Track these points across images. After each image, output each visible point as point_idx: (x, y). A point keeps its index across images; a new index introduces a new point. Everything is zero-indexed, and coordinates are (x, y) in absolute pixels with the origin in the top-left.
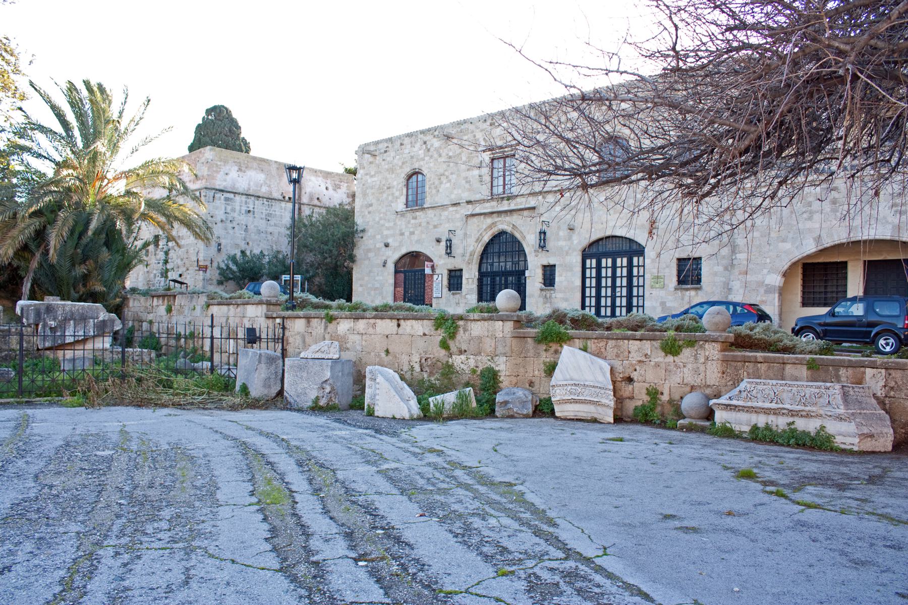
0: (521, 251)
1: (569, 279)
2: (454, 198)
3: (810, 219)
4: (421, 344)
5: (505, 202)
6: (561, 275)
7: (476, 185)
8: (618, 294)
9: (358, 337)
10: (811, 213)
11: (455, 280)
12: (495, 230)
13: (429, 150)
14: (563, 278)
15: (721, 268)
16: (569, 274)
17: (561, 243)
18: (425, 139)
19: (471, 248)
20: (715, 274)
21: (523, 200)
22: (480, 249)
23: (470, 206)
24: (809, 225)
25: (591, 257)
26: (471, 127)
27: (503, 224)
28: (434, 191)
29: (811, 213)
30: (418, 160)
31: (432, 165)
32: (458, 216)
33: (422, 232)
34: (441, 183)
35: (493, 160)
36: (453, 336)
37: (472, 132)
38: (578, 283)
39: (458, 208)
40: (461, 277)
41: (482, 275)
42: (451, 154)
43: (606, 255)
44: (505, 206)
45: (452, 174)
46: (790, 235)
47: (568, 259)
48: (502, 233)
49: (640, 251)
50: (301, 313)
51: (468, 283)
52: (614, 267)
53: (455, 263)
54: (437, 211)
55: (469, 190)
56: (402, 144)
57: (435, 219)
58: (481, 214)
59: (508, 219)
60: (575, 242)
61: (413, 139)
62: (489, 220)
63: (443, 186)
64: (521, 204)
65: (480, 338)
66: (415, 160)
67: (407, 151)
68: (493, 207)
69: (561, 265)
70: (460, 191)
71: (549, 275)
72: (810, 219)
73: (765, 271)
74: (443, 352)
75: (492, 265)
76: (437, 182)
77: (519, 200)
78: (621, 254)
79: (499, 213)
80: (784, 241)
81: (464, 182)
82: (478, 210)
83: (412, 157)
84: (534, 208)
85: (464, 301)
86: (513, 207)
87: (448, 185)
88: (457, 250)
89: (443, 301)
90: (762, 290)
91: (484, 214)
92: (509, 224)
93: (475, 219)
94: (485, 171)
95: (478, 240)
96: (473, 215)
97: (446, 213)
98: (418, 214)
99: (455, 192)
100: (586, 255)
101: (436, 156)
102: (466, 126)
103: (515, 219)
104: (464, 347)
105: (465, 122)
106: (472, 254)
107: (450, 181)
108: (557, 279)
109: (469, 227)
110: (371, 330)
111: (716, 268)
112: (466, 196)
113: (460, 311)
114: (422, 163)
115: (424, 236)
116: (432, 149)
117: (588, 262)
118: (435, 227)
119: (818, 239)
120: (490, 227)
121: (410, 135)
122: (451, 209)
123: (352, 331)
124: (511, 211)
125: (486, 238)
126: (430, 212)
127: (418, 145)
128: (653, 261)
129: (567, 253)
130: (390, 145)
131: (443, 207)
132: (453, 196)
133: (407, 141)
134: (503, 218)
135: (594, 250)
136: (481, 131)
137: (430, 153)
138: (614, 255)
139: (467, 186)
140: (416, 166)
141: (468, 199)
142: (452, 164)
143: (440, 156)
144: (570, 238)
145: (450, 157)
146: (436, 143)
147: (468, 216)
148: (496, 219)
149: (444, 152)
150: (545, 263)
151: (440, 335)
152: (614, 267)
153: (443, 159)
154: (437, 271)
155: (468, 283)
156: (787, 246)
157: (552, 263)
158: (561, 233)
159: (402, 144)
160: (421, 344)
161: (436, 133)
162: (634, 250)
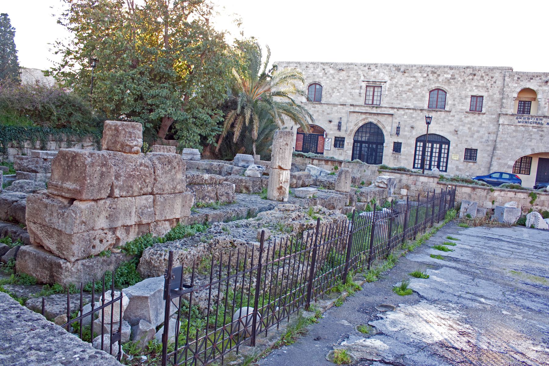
0: (382, 135)
1: (408, 150)
2: (342, 100)
3: (530, 141)
4: (522, 201)
5: (374, 109)
6: (405, 148)
7: (357, 97)
8: (433, 160)
9: (501, 198)
10: (531, 139)
11: (339, 142)
12: (366, 121)
13: (326, 74)
14: (405, 149)
15: (486, 155)
16: (409, 148)
17: (406, 133)
18: (324, 67)
19: (352, 128)
20: (484, 157)
21: (385, 109)
22: (356, 129)
23: (352, 107)
24: (530, 143)
25: (420, 141)
26: (356, 68)
27: (373, 119)
28: (328, 96)
29: (531, 139)
30: (318, 77)
31: (328, 82)
32: (344, 111)
33: (319, 115)
34: (334, 92)
35: (367, 86)
36: (534, 200)
37: (356, 70)
38: (413, 153)
39: (344, 107)
40: (344, 141)
41: (355, 141)
42: (341, 78)
43: (429, 142)
44: (374, 111)
45: (341, 89)
46: (521, 146)
47: (409, 141)
48: (371, 123)
49: (448, 142)
50: (471, 185)
51: (348, 145)
52: (432, 148)
53: (341, 134)
54: (330, 107)
55: (352, 99)
56: (307, 67)
57: (328, 110)
58: (359, 112)
59: (375, 117)
60: (414, 134)
61: (315, 66)
62: (364, 116)
63: (334, 94)
64: (384, 111)
65: (543, 201)
66: (316, 77)
67: (311, 71)
68: (367, 110)
69: (405, 143)
70: (346, 99)
71: (397, 147)
72: (530, 141)
73: (508, 159)
74: (530, 204)
75: (362, 137)
76: (331, 91)
77: (383, 109)
78: (437, 142)
79: (371, 114)
80: (518, 148)
81: (349, 94)
82: (357, 109)
83: (314, 75)
84: (392, 115)
85: (345, 153)
86: (379, 112)
87: (338, 94)
88: (343, 128)
89: (331, 151)
90: (506, 167)
91: (361, 113)
92: (375, 120)
93: (355, 114)
94: (363, 91)
95: (356, 125)
96: (354, 112)
97: (336, 108)
98: (316, 105)
99: (343, 98)
100: (418, 140)
101: (331, 78)
102: (352, 66)
103: (380, 118)
104: (538, 203)
105: (352, 64)
106: (351, 131)
107: (339, 92)
108: (402, 149)
109: (351, 118)
110: (506, 196)
111: (484, 155)
112: (350, 101)
113: (341, 158)
114: (321, 79)
115: (320, 118)
116: (328, 74)
117: (418, 144)
118: (328, 114)
119: (533, 150)
120: (364, 119)
121: (313, 63)
122: (339, 106)
123: (499, 195)
124: (378, 114)
125: (361, 124)
126: (325, 107)
127: (318, 70)
128: (454, 148)
129: (409, 138)
130: (298, 66)
131: (335, 105)
132: (341, 100)
133: (311, 66)
134: (372, 116)
135: (422, 139)
136: (362, 71)
137: (327, 76)
138: (433, 142)
139: (351, 97)
140: (317, 80)
141: (352, 104)
142: (341, 84)
143: (334, 78)
144: (411, 132)
145: (341, 80)
146: (332, 71)
147: (350, 112)
148: (368, 116)
149: (337, 77)
150: (396, 141)
151: (530, 199)
152: (432, 148)
153: (335, 80)
154: (328, 137)
155: (348, 145)
156: (519, 150)
157: (400, 141)
158: (406, 129)
159: (307, 67)
160: (522, 201)
161: (332, 66)
162: (443, 141)
